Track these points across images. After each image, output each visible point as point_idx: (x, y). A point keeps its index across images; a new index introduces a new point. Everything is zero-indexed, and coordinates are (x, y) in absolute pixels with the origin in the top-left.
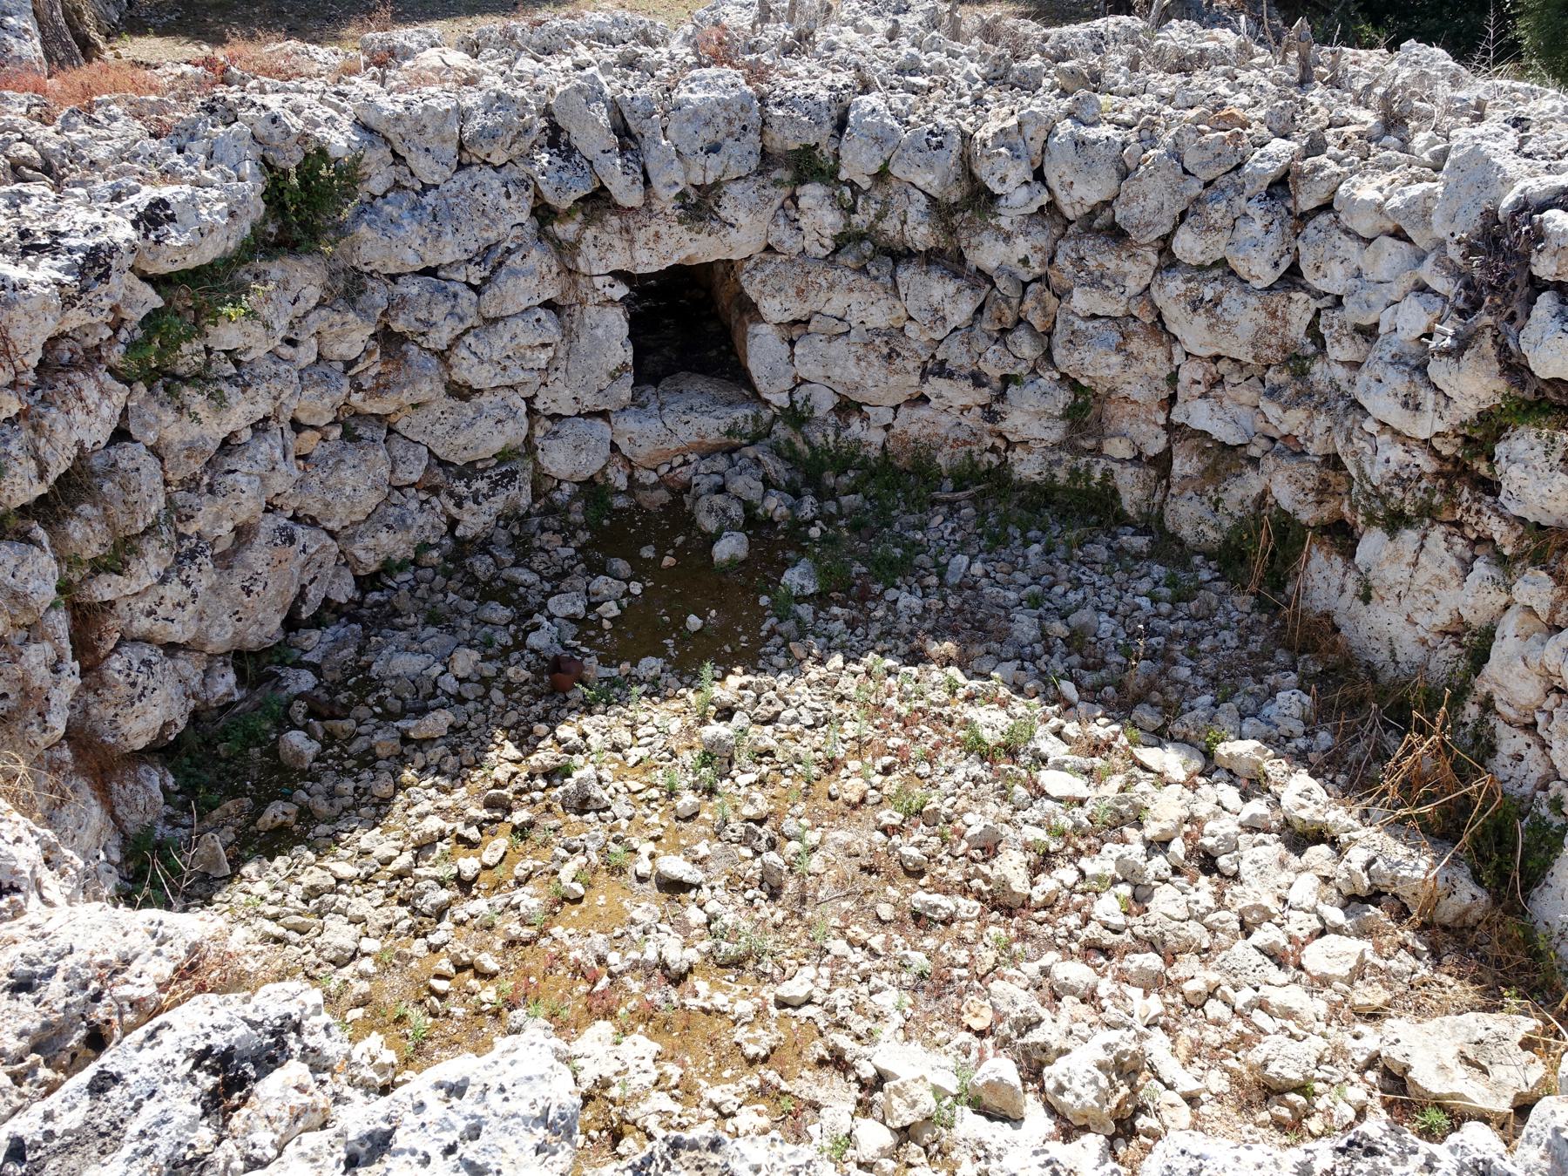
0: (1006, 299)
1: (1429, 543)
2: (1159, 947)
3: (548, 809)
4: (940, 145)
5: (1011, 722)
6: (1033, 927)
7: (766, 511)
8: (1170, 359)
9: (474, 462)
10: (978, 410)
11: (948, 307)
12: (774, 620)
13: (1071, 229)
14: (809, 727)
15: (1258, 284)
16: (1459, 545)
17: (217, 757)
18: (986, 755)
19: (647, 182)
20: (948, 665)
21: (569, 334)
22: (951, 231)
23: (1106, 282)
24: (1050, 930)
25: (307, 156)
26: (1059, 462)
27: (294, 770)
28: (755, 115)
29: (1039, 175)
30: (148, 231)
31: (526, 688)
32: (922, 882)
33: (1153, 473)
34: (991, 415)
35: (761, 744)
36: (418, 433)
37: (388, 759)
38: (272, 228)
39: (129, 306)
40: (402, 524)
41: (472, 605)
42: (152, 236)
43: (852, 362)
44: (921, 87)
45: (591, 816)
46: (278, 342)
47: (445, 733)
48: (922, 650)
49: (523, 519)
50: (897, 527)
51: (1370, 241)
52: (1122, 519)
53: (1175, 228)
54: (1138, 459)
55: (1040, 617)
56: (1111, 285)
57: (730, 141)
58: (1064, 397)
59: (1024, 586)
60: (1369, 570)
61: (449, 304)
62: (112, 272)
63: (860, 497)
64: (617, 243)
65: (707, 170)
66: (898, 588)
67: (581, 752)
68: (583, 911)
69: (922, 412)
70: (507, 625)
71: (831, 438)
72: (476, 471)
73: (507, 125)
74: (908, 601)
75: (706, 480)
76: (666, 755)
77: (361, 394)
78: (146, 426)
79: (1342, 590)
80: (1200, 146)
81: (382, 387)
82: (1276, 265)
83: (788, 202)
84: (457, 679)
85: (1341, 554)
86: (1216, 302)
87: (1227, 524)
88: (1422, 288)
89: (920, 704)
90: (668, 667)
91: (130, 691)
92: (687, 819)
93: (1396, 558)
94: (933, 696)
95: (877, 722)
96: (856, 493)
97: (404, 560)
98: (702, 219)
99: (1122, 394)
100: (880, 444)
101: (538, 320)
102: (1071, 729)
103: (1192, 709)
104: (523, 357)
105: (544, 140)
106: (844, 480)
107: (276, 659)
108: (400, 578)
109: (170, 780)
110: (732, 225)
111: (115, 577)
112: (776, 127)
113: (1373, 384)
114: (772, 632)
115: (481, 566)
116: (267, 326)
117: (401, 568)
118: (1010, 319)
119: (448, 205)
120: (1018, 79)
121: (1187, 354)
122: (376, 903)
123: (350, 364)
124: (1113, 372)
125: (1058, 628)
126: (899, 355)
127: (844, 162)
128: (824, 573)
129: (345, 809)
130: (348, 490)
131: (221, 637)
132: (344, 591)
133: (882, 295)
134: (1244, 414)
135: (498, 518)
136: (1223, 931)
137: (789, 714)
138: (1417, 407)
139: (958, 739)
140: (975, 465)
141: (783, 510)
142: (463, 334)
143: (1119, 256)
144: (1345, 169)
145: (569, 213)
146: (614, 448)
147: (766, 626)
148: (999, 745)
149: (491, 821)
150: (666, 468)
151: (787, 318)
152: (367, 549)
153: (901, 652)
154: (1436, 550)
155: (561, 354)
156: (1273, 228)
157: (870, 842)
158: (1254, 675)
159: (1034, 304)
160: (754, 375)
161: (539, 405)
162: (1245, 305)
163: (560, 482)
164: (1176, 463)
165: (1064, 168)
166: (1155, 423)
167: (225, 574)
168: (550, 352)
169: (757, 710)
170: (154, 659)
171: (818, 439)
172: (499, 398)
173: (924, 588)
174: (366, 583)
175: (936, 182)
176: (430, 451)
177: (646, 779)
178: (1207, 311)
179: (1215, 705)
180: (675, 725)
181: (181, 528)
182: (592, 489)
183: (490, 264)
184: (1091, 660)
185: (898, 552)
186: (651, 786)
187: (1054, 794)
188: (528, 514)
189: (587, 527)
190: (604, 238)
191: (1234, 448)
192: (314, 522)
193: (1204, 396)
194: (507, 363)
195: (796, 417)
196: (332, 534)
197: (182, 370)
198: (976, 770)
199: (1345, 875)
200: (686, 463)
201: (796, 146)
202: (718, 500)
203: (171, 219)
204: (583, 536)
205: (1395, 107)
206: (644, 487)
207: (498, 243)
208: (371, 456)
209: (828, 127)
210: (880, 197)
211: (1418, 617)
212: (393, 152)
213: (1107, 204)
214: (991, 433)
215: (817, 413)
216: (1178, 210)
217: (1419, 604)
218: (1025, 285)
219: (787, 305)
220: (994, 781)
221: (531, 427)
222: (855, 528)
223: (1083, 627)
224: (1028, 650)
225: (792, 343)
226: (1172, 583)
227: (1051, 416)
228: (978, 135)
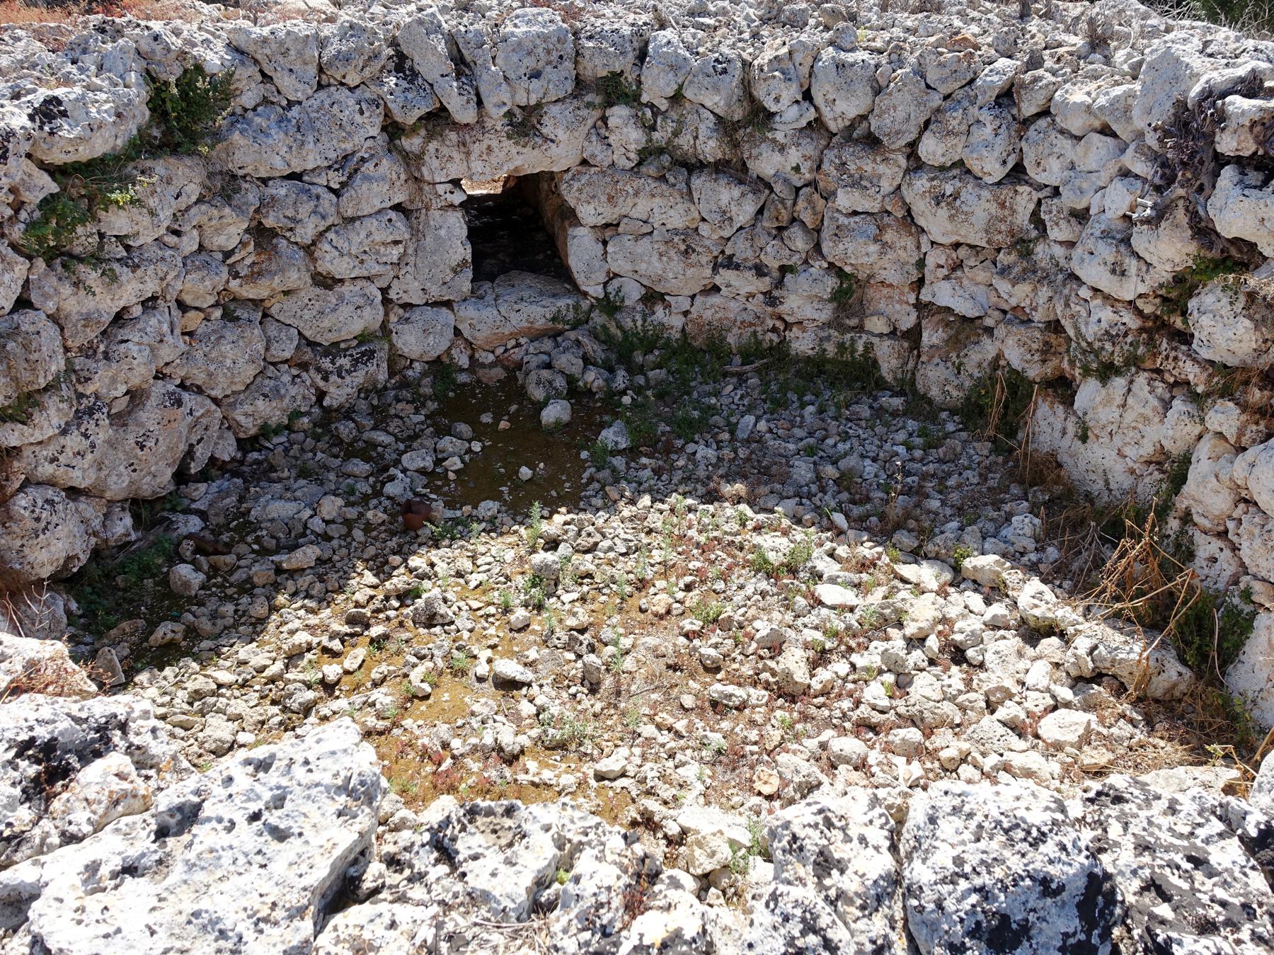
0: (782, 201)
1: (1135, 387)
2: (918, 723)
3: (401, 624)
4: (725, 71)
5: (792, 545)
6: (813, 710)
7: (586, 383)
8: (919, 247)
9: (338, 343)
10: (761, 297)
11: (734, 209)
12: (593, 470)
13: (835, 140)
14: (622, 555)
15: (989, 180)
16: (1160, 388)
17: (117, 588)
18: (771, 573)
19: (480, 103)
20: (739, 503)
21: (416, 233)
22: (736, 145)
23: (864, 183)
24: (827, 713)
25: (186, 71)
26: (828, 338)
27: (182, 597)
28: (569, 46)
29: (807, 96)
30: (43, 123)
31: (383, 528)
32: (719, 676)
33: (906, 345)
34: (771, 300)
35: (582, 568)
36: (289, 317)
37: (264, 587)
38: (156, 133)
39: (28, 190)
40: (276, 394)
41: (338, 462)
42: (47, 128)
43: (655, 258)
44: (708, 26)
45: (437, 630)
46: (163, 231)
47: (313, 564)
48: (716, 491)
49: (381, 392)
50: (695, 395)
51: (1079, 138)
52: (881, 385)
53: (921, 134)
54: (893, 333)
55: (815, 463)
56: (869, 185)
57: (549, 69)
58: (831, 283)
59: (801, 440)
60: (1085, 414)
61: (312, 204)
62: (10, 154)
63: (664, 371)
64: (455, 155)
65: (529, 93)
66: (696, 443)
67: (429, 578)
68: (430, 706)
69: (715, 300)
70: (367, 478)
71: (639, 323)
72: (340, 350)
73: (360, 52)
74: (705, 452)
75: (535, 359)
76: (502, 579)
77: (238, 281)
78: (46, 297)
79: (1064, 432)
80: (940, 64)
81: (256, 275)
82: (1004, 162)
83: (600, 123)
84: (324, 521)
85: (1063, 403)
86: (956, 196)
87: (968, 384)
88: (1125, 174)
89: (715, 534)
90: (504, 508)
91: (35, 525)
92: (519, 630)
93: (1108, 401)
94: (726, 528)
95: (680, 549)
96: (661, 368)
97: (279, 425)
98: (527, 135)
99: (879, 279)
100: (680, 327)
101: (390, 220)
102: (842, 551)
103: (942, 533)
104: (378, 253)
105: (391, 65)
106: (650, 358)
107: (168, 506)
108: (276, 440)
109: (74, 606)
110: (552, 141)
111: (20, 426)
112: (587, 57)
113: (1087, 256)
114: (591, 479)
115: (345, 429)
116: (152, 213)
117: (277, 432)
118: (786, 218)
119: (310, 119)
120: (789, 19)
121: (933, 243)
122: (252, 704)
123: (228, 254)
124: (871, 260)
125: (830, 471)
126: (694, 251)
127: (645, 86)
128: (633, 431)
129: (226, 628)
130: (229, 363)
131: (118, 485)
132: (227, 450)
133: (679, 200)
134: (980, 291)
135: (360, 391)
136: (972, 709)
137: (605, 544)
138: (1123, 273)
139: (748, 561)
140: (759, 343)
141: (600, 382)
142: (326, 231)
143: (875, 160)
144: (1060, 79)
145: (414, 130)
146: (457, 332)
147: (586, 475)
148: (782, 564)
149: (352, 635)
150: (501, 350)
151: (601, 221)
152: (246, 415)
153: (699, 493)
154: (1141, 394)
155: (410, 251)
156: (1001, 131)
157: (675, 645)
158: (993, 504)
159: (805, 205)
160: (574, 270)
161: (392, 295)
162: (979, 197)
163: (412, 361)
164: (925, 335)
165: (827, 87)
166: (907, 303)
167: (121, 431)
168: (401, 248)
169: (579, 541)
170: (56, 499)
171: (628, 323)
172: (358, 288)
173: (718, 442)
174: (245, 445)
175: (722, 103)
176: (300, 333)
177: (484, 598)
178: (948, 204)
179: (961, 529)
180: (509, 555)
181: (80, 389)
182: (439, 367)
183: (347, 170)
184: (858, 497)
185: (696, 414)
186: (489, 604)
187: (829, 603)
188: (385, 388)
189: (434, 397)
190: (445, 151)
191: (972, 320)
192: (200, 390)
193: (947, 278)
194: (364, 257)
195: (610, 306)
196: (216, 401)
197: (78, 250)
198: (764, 585)
199: (1073, 660)
200: (518, 345)
201: (604, 73)
202: (546, 374)
203: (64, 114)
204: (432, 406)
205: (1099, 30)
206: (483, 366)
207: (354, 153)
208: (248, 334)
209: (631, 57)
210: (675, 117)
211: (1127, 451)
212: (261, 71)
213: (863, 118)
214: (772, 316)
215: (627, 303)
216: (922, 120)
217: (1128, 440)
218: (798, 189)
219: (600, 210)
220: (778, 594)
221: (386, 314)
222: (660, 396)
223: (851, 470)
224: (805, 489)
225: (605, 243)
226: (923, 433)
227: (821, 300)
228: (756, 63)
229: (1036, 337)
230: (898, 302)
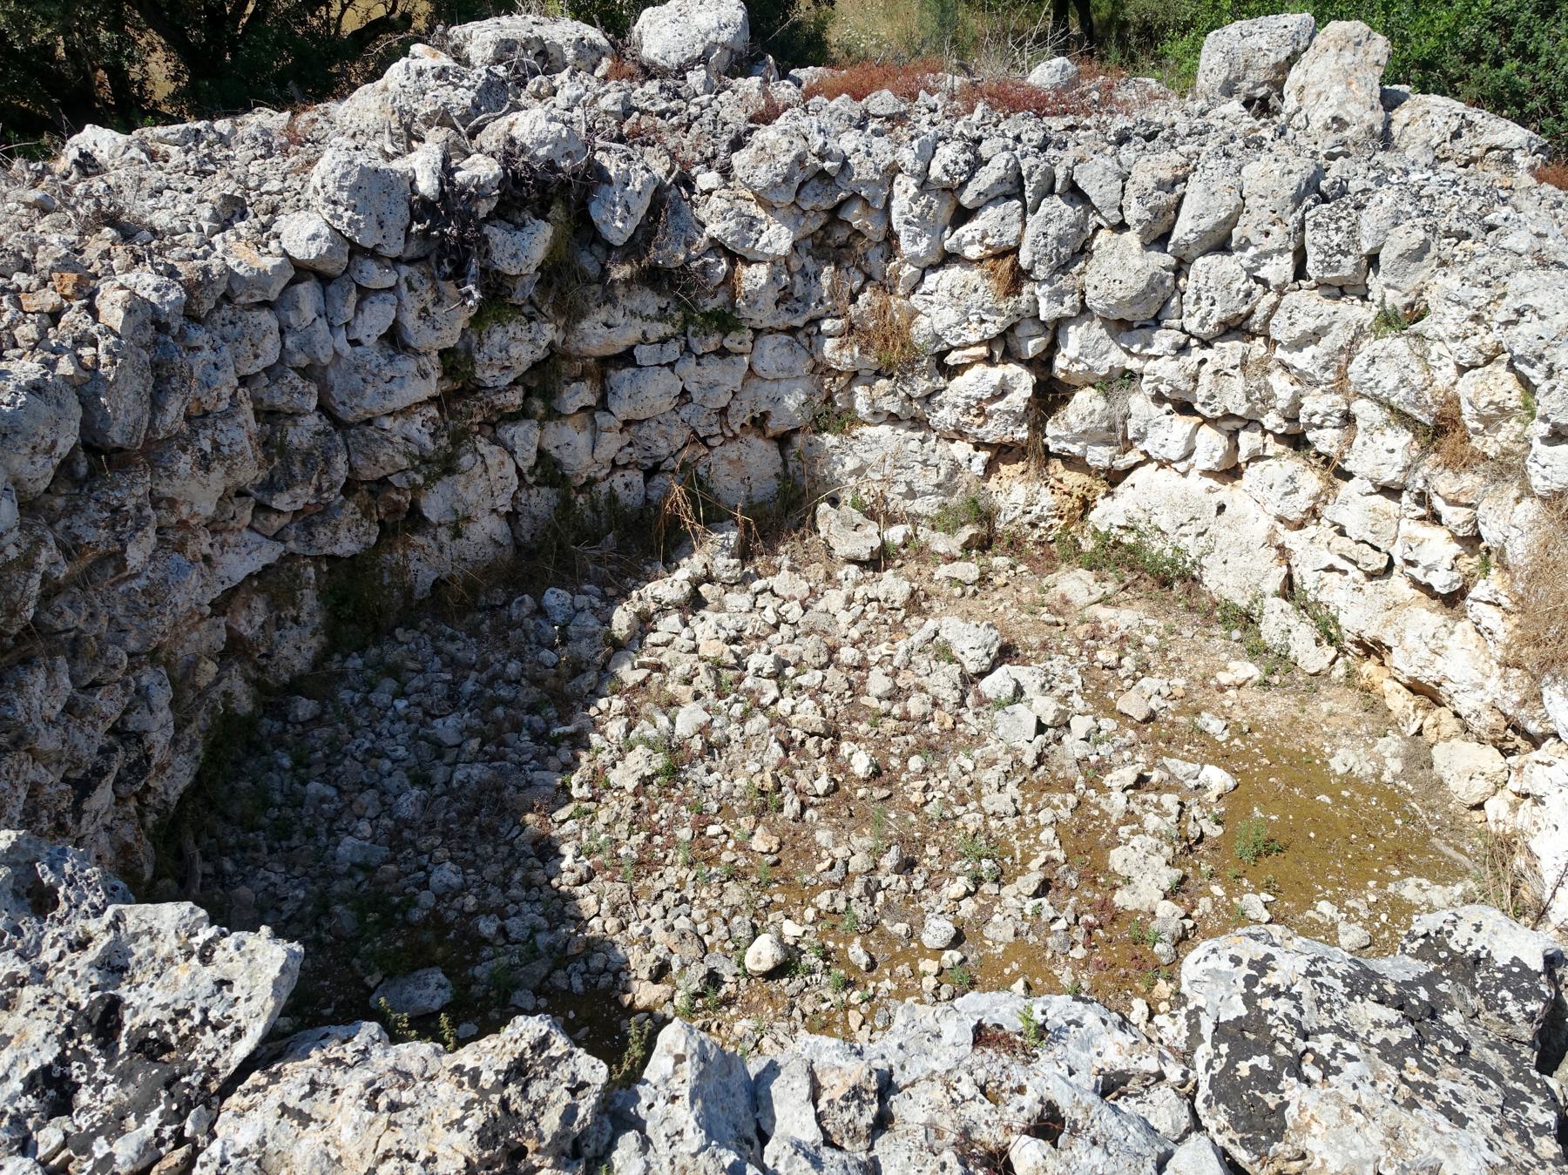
86: (216, 446)
229: (349, 512)
230: (189, 631)
